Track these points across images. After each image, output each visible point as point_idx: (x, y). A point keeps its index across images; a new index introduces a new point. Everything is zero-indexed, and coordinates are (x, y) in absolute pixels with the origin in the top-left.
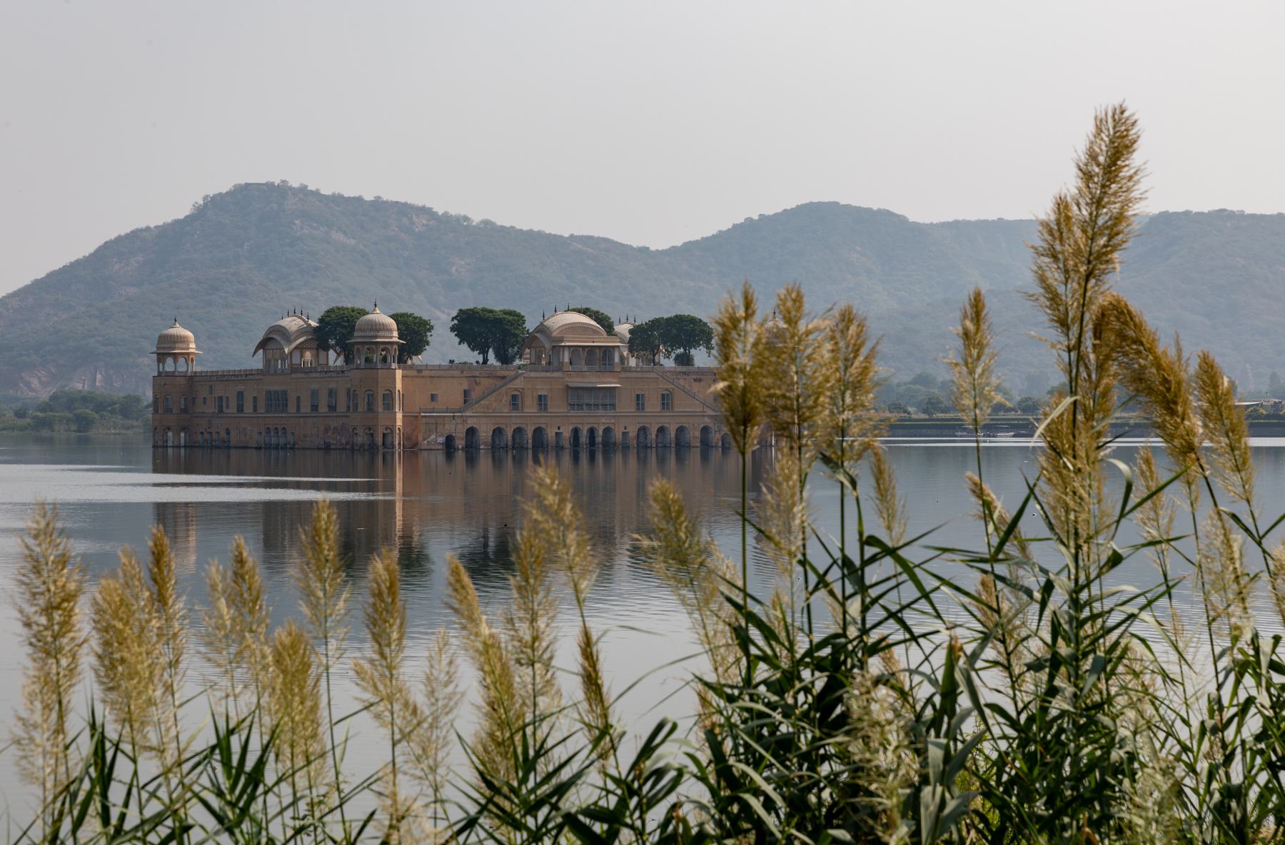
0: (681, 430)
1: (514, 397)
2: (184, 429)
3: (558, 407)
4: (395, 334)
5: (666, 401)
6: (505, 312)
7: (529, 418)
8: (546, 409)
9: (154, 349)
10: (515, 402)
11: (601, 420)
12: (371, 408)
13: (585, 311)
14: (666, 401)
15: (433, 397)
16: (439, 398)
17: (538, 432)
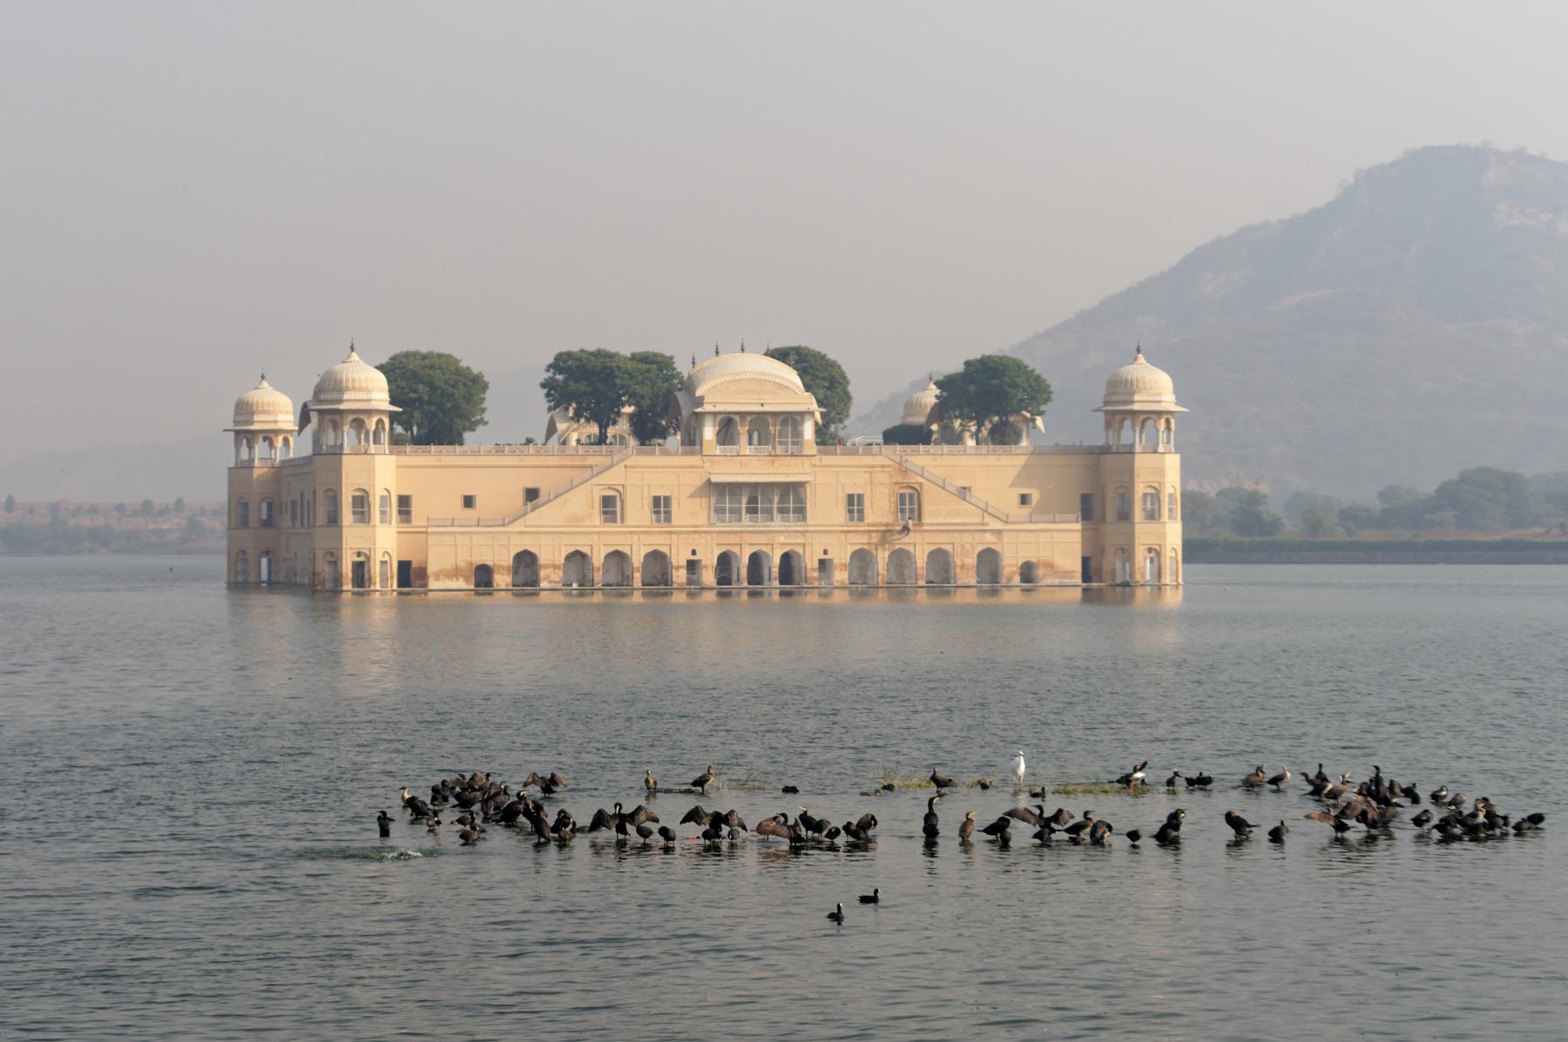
0: (940, 559)
1: (608, 502)
2: (267, 553)
3: (690, 512)
4: (386, 396)
5: (910, 504)
6: (634, 357)
7: (637, 537)
8: (668, 519)
9: (230, 426)
10: (609, 506)
11: (772, 537)
12: (334, 519)
13: (781, 355)
14: (910, 504)
15: (469, 502)
16: (478, 502)
17: (657, 559)
